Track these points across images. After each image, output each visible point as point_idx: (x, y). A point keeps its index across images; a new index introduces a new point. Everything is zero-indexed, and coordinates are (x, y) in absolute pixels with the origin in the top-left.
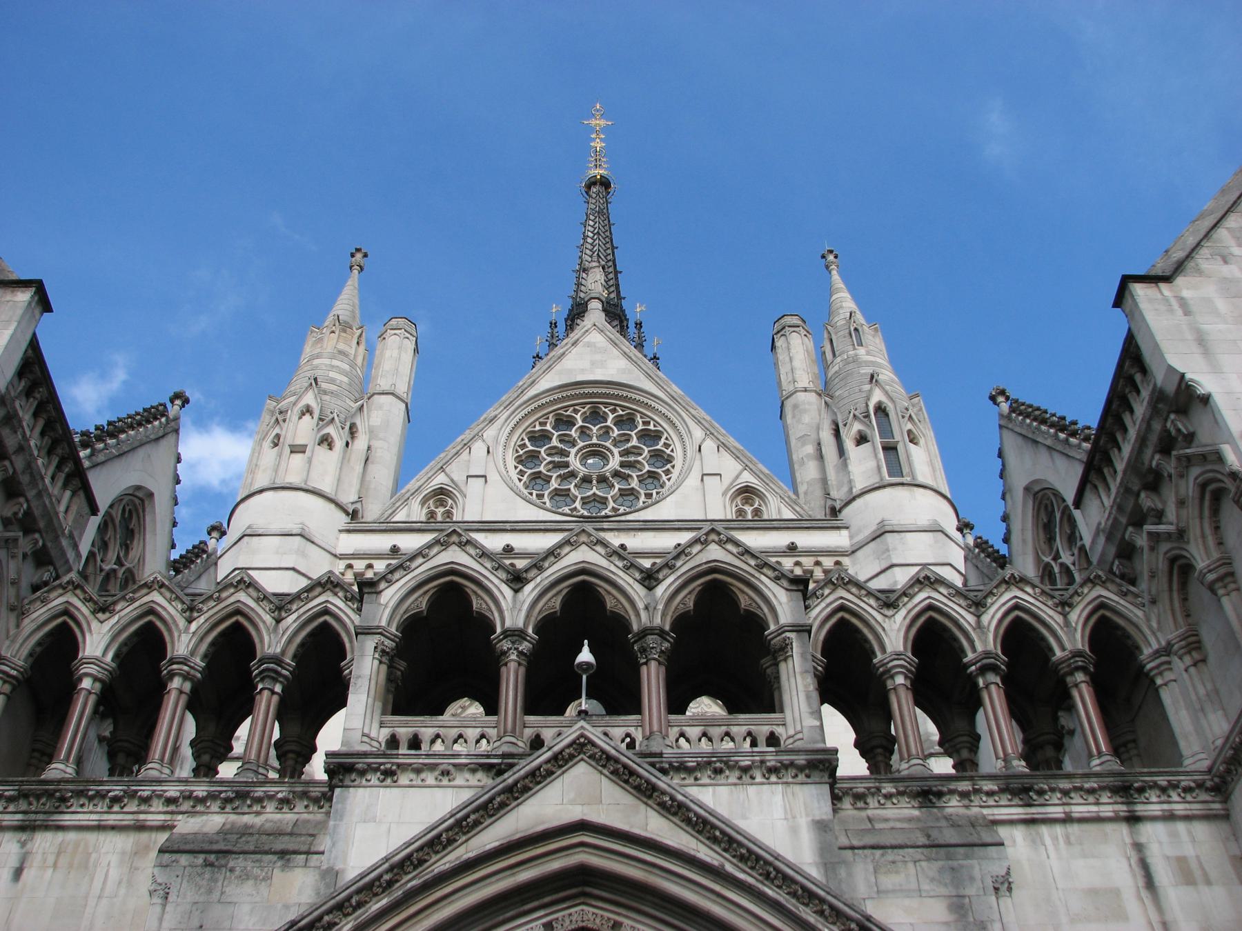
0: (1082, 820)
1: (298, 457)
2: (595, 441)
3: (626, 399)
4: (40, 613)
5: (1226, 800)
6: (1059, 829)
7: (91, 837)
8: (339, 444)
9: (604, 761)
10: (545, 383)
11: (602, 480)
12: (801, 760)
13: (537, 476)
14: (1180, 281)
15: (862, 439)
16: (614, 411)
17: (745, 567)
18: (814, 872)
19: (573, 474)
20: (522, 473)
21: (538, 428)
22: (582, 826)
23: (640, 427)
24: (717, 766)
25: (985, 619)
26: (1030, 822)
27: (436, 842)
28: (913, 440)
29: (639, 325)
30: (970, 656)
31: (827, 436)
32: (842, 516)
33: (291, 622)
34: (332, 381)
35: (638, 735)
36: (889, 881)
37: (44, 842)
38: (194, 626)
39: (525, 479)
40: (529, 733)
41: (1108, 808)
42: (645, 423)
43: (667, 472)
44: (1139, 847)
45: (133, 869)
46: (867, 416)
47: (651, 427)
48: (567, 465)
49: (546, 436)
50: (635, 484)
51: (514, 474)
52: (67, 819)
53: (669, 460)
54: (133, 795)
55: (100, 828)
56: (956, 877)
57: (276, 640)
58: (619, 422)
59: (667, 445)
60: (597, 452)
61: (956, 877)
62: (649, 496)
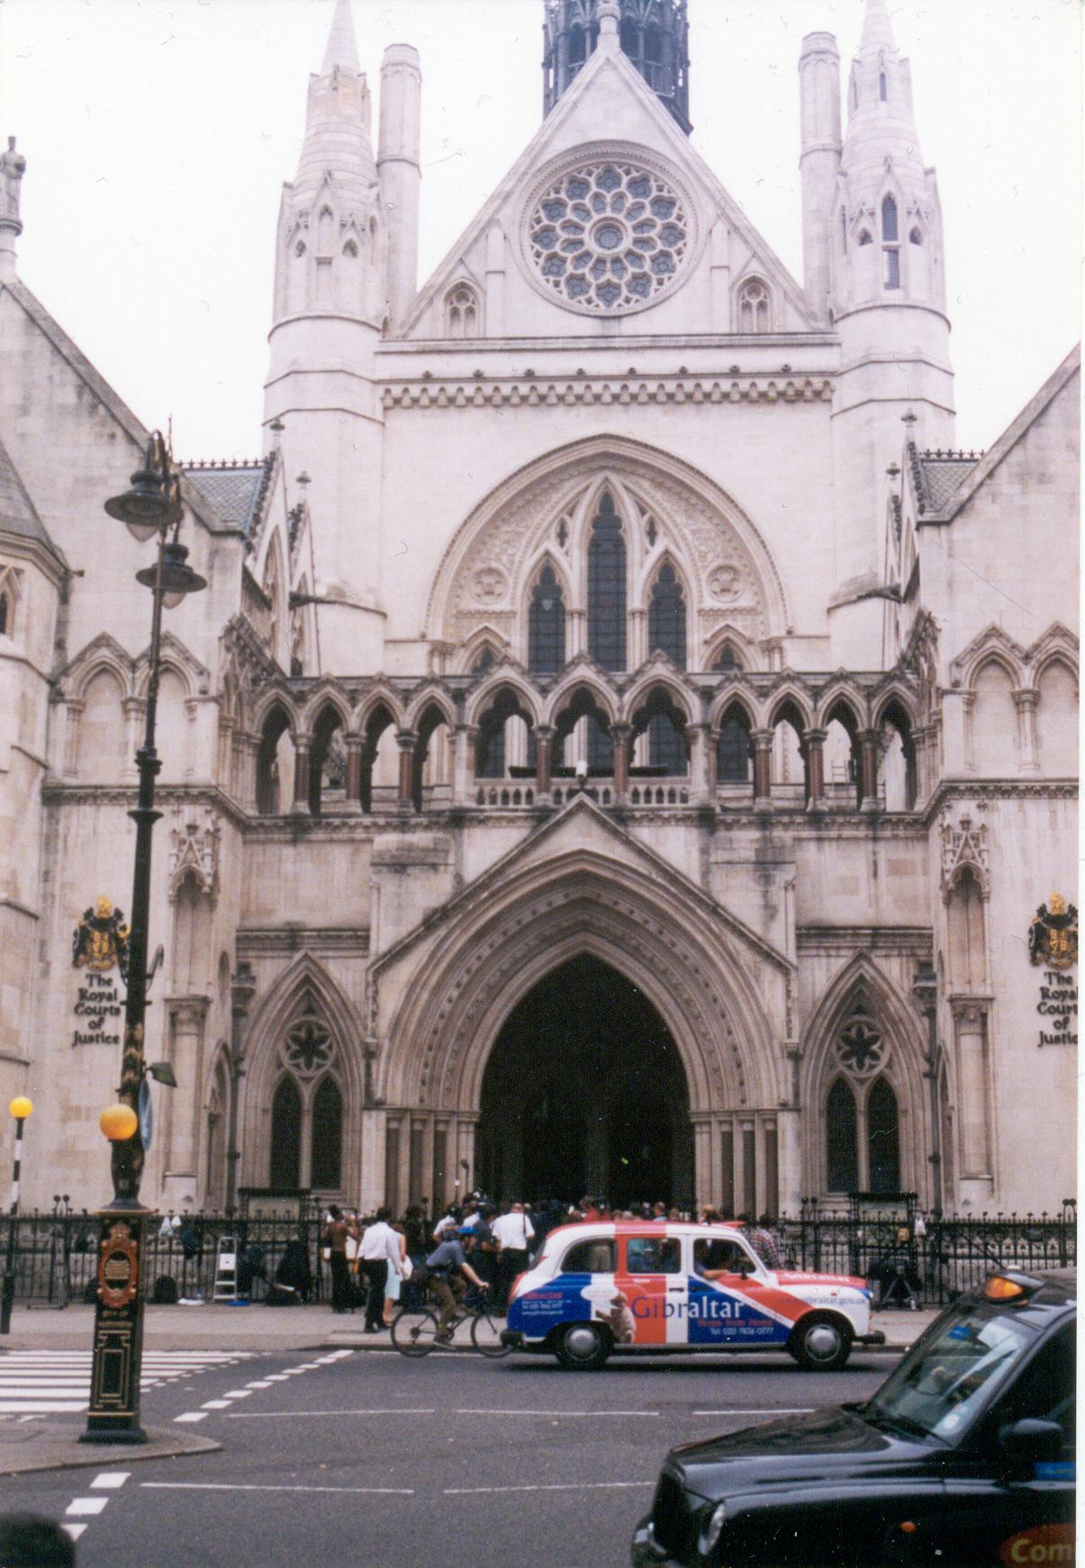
1: (324, 268)
2: (609, 213)
3: (640, 159)
4: (263, 703)
6: (834, 844)
8: (361, 251)
9: (593, 814)
11: (616, 260)
12: (694, 813)
13: (553, 256)
14: (958, 522)
15: (865, 238)
16: (628, 173)
18: (696, 878)
19: (588, 254)
20: (538, 255)
21: (553, 196)
22: (582, 852)
23: (654, 193)
24: (653, 818)
25: (820, 704)
26: (820, 839)
27: (510, 861)
28: (915, 238)
31: (836, 220)
32: (840, 326)
33: (414, 705)
35: (611, 788)
36: (733, 883)
37: (302, 848)
38: (357, 710)
39: (541, 261)
40: (553, 788)
41: (862, 833)
42: (660, 189)
43: (679, 252)
44: (875, 853)
45: (353, 863)
47: (665, 193)
48: (581, 242)
49: (560, 204)
50: (647, 267)
51: (531, 258)
52: (313, 837)
53: (682, 235)
54: (345, 824)
55: (331, 841)
56: (766, 880)
57: (407, 717)
58: (633, 184)
59: (680, 218)
60: (608, 230)
61: (766, 880)
62: (660, 282)
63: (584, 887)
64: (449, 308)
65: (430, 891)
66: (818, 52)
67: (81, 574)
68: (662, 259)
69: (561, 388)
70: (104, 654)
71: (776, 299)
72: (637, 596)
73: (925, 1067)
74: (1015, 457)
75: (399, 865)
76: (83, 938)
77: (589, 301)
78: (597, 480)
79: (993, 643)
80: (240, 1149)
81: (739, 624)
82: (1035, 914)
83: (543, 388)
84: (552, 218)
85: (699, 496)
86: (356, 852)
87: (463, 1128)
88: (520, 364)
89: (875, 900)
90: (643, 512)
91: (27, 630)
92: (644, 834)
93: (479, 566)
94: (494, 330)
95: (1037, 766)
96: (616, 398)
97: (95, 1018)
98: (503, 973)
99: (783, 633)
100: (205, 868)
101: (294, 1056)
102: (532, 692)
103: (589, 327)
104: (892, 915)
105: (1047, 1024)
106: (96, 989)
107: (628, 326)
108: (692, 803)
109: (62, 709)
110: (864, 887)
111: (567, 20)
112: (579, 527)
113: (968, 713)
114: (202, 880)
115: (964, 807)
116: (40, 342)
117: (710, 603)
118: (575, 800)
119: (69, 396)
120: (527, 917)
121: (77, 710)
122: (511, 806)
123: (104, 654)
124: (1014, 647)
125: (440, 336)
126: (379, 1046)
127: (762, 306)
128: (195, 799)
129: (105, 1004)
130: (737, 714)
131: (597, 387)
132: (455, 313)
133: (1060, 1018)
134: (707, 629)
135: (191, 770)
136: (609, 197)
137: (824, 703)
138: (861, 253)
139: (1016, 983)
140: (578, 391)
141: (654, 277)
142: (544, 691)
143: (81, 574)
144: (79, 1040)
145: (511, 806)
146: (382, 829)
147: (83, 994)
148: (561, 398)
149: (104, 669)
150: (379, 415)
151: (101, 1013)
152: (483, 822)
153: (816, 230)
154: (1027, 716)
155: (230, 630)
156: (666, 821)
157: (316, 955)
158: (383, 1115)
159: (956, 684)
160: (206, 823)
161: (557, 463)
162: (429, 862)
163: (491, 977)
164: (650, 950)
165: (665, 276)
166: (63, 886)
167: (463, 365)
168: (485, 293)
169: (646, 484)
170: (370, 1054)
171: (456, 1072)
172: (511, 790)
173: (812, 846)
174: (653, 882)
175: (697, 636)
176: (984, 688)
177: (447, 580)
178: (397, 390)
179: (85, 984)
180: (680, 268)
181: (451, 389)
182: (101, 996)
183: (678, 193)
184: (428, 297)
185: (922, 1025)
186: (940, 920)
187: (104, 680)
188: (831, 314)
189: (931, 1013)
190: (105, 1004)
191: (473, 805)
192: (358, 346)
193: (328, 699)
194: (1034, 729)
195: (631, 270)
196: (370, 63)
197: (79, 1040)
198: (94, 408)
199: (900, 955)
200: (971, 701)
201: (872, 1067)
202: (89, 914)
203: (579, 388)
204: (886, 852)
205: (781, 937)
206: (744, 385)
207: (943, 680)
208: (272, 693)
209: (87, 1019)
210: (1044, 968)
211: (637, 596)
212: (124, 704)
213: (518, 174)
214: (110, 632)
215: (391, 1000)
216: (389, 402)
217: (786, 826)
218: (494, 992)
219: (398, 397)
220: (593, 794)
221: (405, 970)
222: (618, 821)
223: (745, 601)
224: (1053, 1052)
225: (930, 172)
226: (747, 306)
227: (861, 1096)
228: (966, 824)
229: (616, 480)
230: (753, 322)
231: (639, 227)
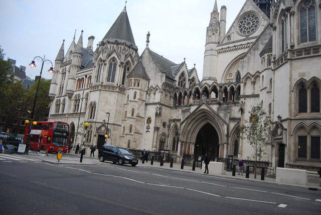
37: (177, 110)
58: (252, 16)
60: (249, 23)
65: (188, 114)
76: (148, 120)
91: (141, 86)
92: (211, 106)
100: (158, 112)
103: (245, 38)
107: (250, 37)
120: (198, 117)
130: (226, 88)
142: (201, 88)
150: (217, 54)
155: (163, 84)
156: (214, 104)
177: (224, 75)
192: (214, 46)
194: (254, 87)
203: (241, 47)
205: (227, 120)
213: (236, 19)
215: (182, 128)
222: (208, 104)
228: (242, 102)
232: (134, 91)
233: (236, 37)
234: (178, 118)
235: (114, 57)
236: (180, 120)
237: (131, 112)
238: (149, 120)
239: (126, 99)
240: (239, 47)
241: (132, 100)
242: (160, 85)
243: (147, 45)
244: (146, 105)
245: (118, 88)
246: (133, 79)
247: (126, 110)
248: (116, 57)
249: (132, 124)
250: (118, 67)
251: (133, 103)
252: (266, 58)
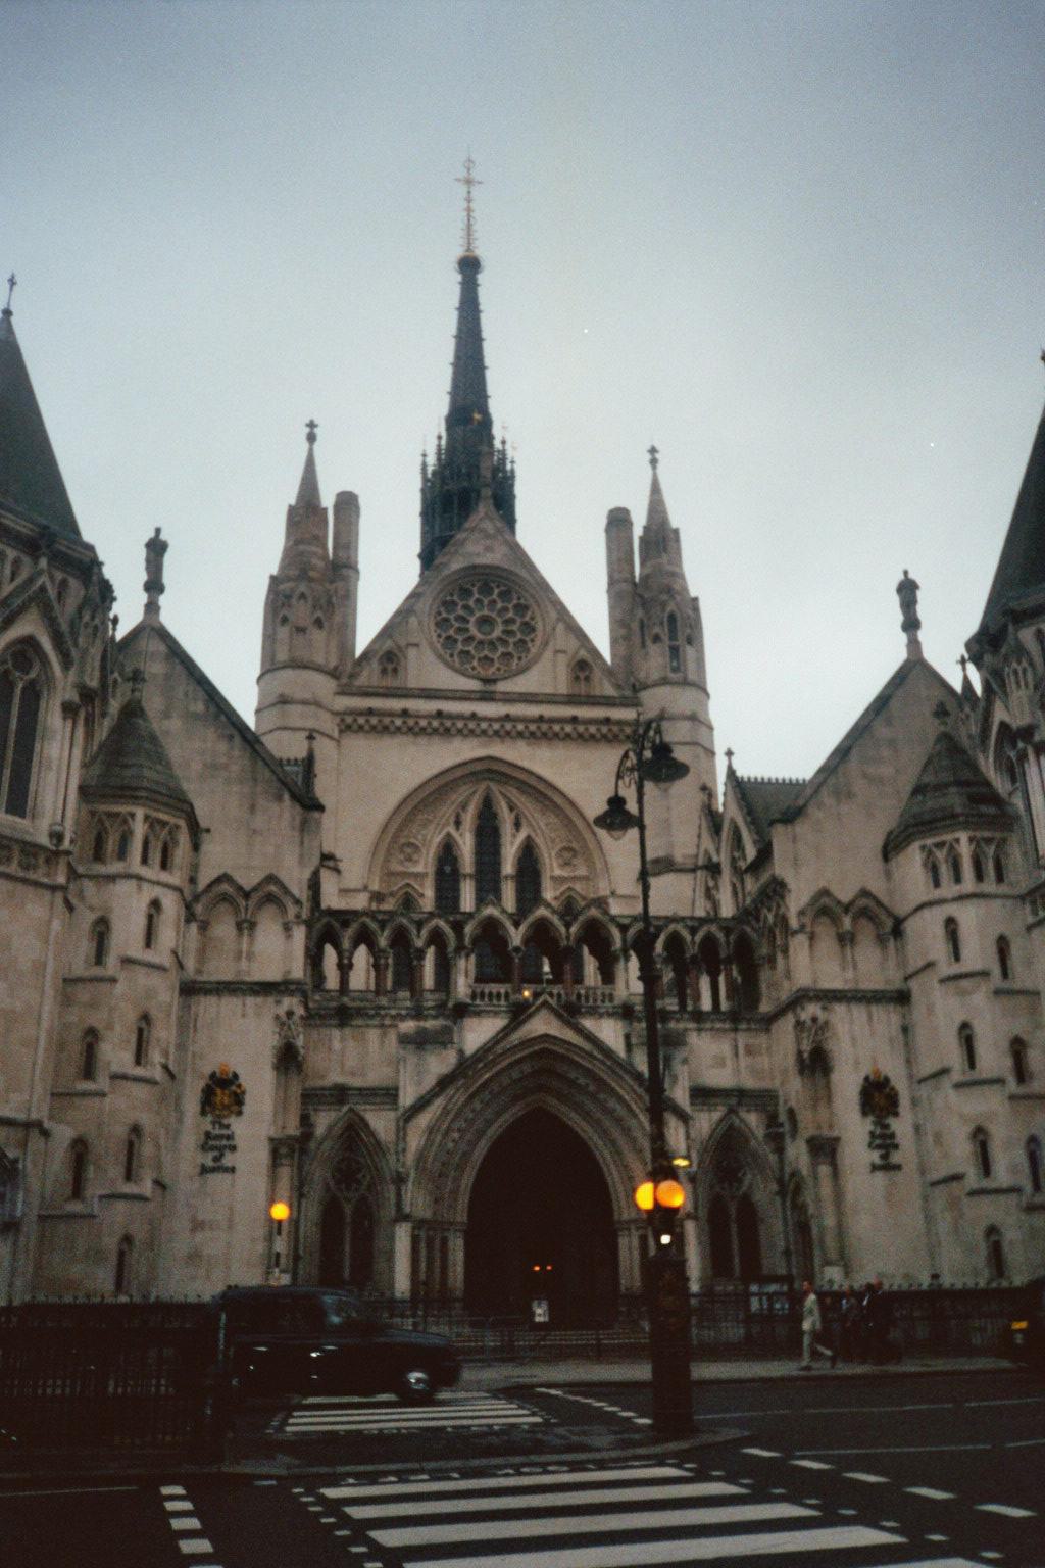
0: (718, 1030)
2: (486, 612)
3: (507, 579)
4: (319, 926)
5: (770, 1024)
6: (708, 1033)
7: (363, 1029)
8: (326, 624)
10: (456, 564)
13: (449, 638)
15: (657, 639)
16: (498, 586)
17: (605, 919)
18: (622, 1053)
19: (471, 639)
20: (439, 636)
21: (448, 598)
22: (547, 1036)
23: (515, 602)
24: (593, 1012)
26: (699, 1030)
29: (504, 442)
30: (687, 956)
31: (635, 626)
34: (313, 568)
35: (562, 992)
37: (347, 1031)
41: (727, 1026)
42: (519, 599)
43: (532, 641)
44: (735, 1040)
46: (662, 623)
47: (522, 601)
48: (467, 630)
49: (454, 604)
51: (434, 638)
53: (533, 630)
54: (377, 1014)
55: (368, 1026)
58: (501, 595)
59: (532, 618)
60: (485, 621)
62: (520, 659)
63: (547, 1058)
64: (380, 667)
65: (439, 1063)
66: (618, 521)
67: (208, 831)
68: (521, 644)
69: (460, 724)
70: (225, 887)
71: (597, 674)
72: (508, 867)
73: (774, 1187)
74: (832, 781)
75: (420, 1042)
77: (473, 668)
78: (482, 787)
79: (825, 901)
80: (301, 1252)
81: (578, 887)
82: (861, 1081)
83: (448, 723)
84: (448, 612)
85: (552, 801)
86: (384, 1035)
87: (458, 1234)
88: (431, 706)
89: (737, 1071)
90: (511, 809)
92: (588, 1023)
93: (403, 841)
94: (413, 682)
95: (857, 982)
96: (496, 733)
97: (216, 1153)
98: (486, 1121)
99: (608, 893)
101: (338, 1183)
102: (509, 925)
103: (474, 685)
104: (749, 1083)
105: (875, 1156)
106: (218, 1131)
107: (501, 687)
108: (617, 1002)
109: (194, 927)
110: (729, 1062)
111: (442, 487)
112: (469, 818)
113: (811, 946)
114: (297, 1052)
115: (812, 1009)
116: (178, 667)
117: (558, 872)
118: (541, 1000)
119: (200, 707)
121: (204, 927)
122: (495, 1002)
123: (225, 887)
124: (839, 903)
125: (375, 684)
126: (408, 1175)
127: (587, 679)
128: (291, 994)
129: (224, 1143)
131: (484, 725)
132: (384, 671)
133: (883, 1152)
134: (555, 890)
135: (289, 972)
136: (486, 602)
137: (698, 938)
138: (654, 650)
139: (854, 1129)
140: (470, 727)
141: (516, 655)
142: (517, 924)
143: (208, 831)
144: (204, 1170)
145: (495, 1002)
146: (403, 1018)
147: (208, 1135)
148: (460, 731)
149: (224, 898)
150: (336, 734)
151: (221, 1151)
152: (478, 1014)
153: (622, 632)
154: (848, 947)
156: (601, 1016)
157: (360, 1108)
158: (410, 1225)
159: (803, 927)
160: (300, 1011)
161: (459, 773)
162: (441, 1040)
163: (479, 1124)
164: (590, 1105)
165: (523, 655)
166: (194, 1055)
167: (396, 705)
168: (406, 658)
169: (515, 791)
170: (400, 1180)
171: (455, 1193)
172: (494, 991)
173: (695, 1034)
174: (595, 1058)
175: (549, 893)
176: (819, 929)
178: (349, 720)
179: (209, 1128)
180: (533, 650)
181: (387, 720)
182: (221, 1137)
183: (531, 602)
184: (366, 655)
185: (773, 1158)
186: (793, 1089)
187: (224, 907)
188: (634, 686)
189: (780, 1151)
190: (224, 1143)
191: (469, 1001)
192: (323, 686)
193: (364, 926)
195: (501, 650)
196: (328, 501)
197: (204, 1170)
198: (217, 717)
199: (757, 1110)
200: (812, 938)
201: (737, 1189)
202: (213, 1076)
203: (472, 725)
204: (742, 1039)
206: (581, 728)
207: (794, 923)
208: (325, 920)
209: (211, 1155)
210: (870, 1119)
211: (508, 867)
212: (239, 926)
214: (229, 871)
215: (415, 1141)
216: (343, 727)
217: (677, 1020)
218: (480, 1134)
219: (351, 725)
220: (551, 995)
221: (424, 1119)
222: (570, 1012)
223: (582, 871)
224: (879, 1175)
225: (695, 600)
226: (577, 678)
227: (733, 1210)
228: (815, 1019)
229: (494, 787)
230: (582, 689)
231: (508, 622)
232: (149, 893)
233: (428, 669)
234: (357, 1082)
235: (29, 642)
236: (389, 1095)
237: (133, 1039)
238: (222, 1093)
239: (86, 947)
240: (460, 724)
241: (136, 950)
242: (296, 879)
243: (152, 608)
244: (190, 990)
245: (63, 861)
246: (140, 813)
247: (96, 1019)
248: (47, 645)
249: (146, 1120)
250: (53, 718)
251: (143, 979)
252: (965, 850)
